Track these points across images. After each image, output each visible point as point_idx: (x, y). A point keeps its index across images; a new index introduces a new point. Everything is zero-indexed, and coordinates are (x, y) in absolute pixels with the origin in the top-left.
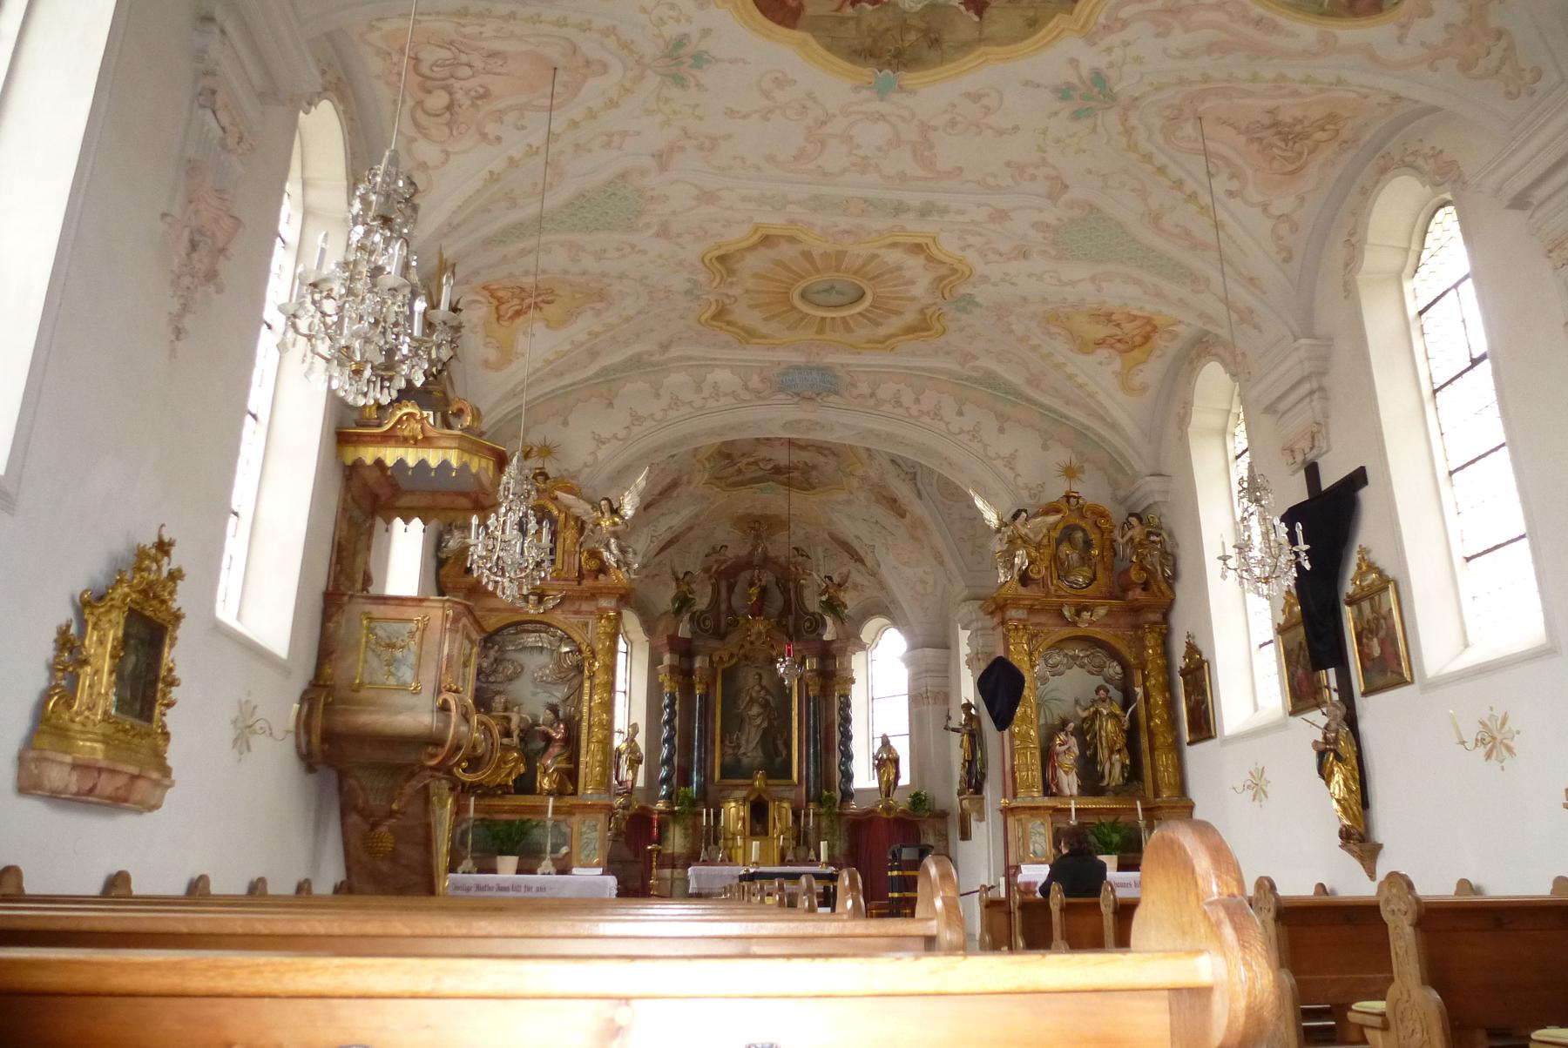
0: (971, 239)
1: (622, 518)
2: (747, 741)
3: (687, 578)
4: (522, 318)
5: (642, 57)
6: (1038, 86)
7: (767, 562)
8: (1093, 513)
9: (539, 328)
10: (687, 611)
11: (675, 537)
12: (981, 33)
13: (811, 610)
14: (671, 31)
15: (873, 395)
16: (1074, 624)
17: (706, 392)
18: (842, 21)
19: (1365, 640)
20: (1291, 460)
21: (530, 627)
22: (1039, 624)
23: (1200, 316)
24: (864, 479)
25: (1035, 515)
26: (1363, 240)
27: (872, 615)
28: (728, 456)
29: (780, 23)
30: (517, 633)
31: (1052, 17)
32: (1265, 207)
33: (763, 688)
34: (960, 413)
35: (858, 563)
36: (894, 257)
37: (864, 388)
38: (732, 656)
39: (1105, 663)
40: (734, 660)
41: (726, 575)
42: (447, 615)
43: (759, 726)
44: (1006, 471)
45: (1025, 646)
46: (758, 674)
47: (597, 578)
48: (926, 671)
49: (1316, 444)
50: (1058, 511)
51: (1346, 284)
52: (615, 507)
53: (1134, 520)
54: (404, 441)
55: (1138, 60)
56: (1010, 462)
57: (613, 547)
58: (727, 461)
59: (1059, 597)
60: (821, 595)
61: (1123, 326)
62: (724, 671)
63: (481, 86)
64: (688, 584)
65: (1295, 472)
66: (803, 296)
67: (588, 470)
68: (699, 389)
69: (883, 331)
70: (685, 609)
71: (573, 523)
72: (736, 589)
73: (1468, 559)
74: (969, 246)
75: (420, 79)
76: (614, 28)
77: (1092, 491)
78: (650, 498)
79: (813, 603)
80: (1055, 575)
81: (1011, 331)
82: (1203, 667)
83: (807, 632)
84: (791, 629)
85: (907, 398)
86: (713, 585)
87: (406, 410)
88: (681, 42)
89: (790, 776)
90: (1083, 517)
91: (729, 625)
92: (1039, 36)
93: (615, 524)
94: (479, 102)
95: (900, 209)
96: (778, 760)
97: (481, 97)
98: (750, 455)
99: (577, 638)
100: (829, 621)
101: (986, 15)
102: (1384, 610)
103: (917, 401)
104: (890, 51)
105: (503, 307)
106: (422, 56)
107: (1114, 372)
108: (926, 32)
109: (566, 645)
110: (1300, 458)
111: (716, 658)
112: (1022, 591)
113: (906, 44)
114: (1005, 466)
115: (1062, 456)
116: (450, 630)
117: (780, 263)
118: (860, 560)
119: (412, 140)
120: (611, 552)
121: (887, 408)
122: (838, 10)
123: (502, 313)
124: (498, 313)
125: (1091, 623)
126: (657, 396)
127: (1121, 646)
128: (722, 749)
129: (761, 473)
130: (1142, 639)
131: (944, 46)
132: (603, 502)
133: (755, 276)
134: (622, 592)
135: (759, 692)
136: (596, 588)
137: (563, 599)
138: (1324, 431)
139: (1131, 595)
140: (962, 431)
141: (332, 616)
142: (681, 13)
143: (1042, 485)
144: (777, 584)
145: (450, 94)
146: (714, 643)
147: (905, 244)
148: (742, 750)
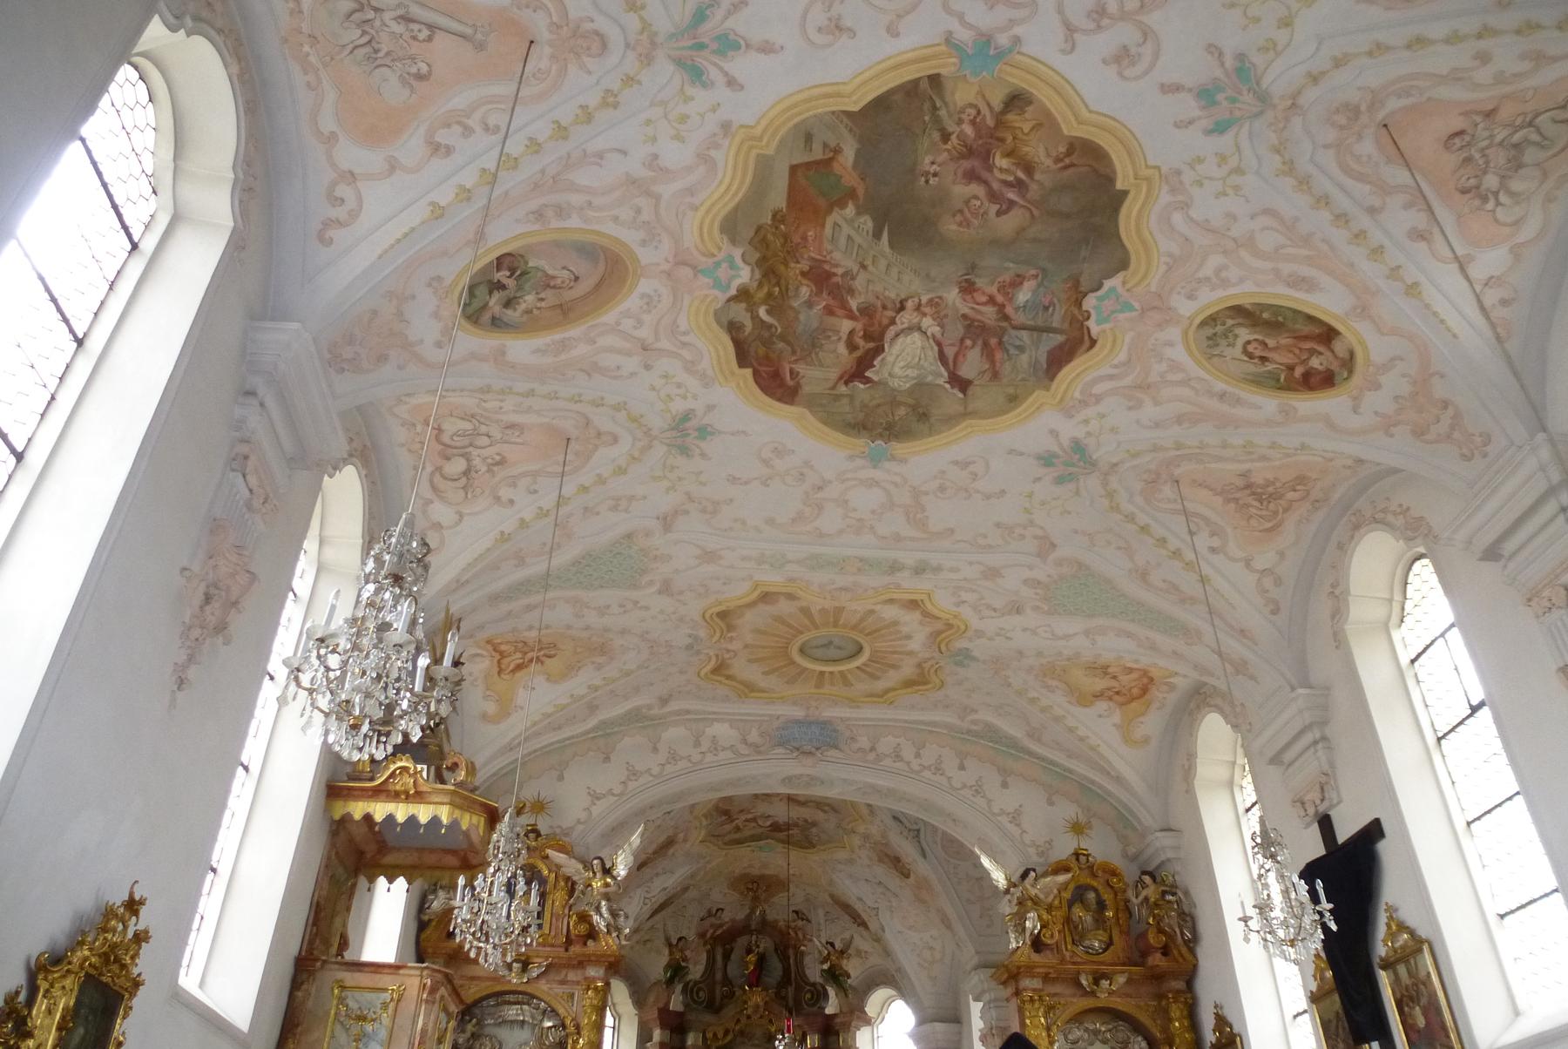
0: (965, 596)
1: (614, 878)
3: (681, 944)
5: (650, 430)
6: (1022, 454)
7: (765, 926)
8: (1104, 871)
9: (540, 680)
10: (679, 982)
11: (670, 898)
12: (965, 408)
13: (812, 980)
14: (678, 406)
15: (873, 749)
16: (1093, 994)
17: (705, 745)
18: (837, 397)
19: (1406, 1009)
20: (1303, 813)
21: (512, 998)
22: (1055, 995)
23: (1196, 667)
24: (866, 837)
25: (1045, 875)
26: (1347, 592)
27: (878, 985)
28: (726, 813)
29: (779, 400)
30: (498, 1005)
31: (1031, 394)
32: (1248, 563)
34: (962, 767)
35: (861, 928)
36: (890, 613)
37: (864, 742)
38: (727, 1032)
39: (1129, 1038)
40: (729, 1038)
41: (722, 940)
42: (425, 985)
44: (1011, 828)
45: (1042, 1020)
47: (585, 944)
49: (1327, 795)
50: (1067, 870)
51: (1335, 634)
52: (608, 867)
53: (1147, 879)
54: (396, 796)
55: (1113, 430)
56: (1016, 817)
57: (604, 910)
58: (724, 818)
59: (1074, 963)
60: (822, 963)
61: (1121, 678)
63: (498, 454)
64: (682, 951)
65: (1308, 825)
66: (802, 651)
67: (581, 827)
68: (697, 744)
69: (881, 685)
70: (677, 979)
71: (562, 884)
72: (733, 957)
73: (1502, 917)
74: (964, 602)
75: (441, 447)
76: (625, 403)
77: (1101, 847)
78: (644, 857)
79: (814, 972)
80: (1069, 939)
81: (1009, 685)
82: (1235, 1042)
84: (791, 1003)
85: (908, 753)
86: (708, 952)
87: (400, 764)
88: (687, 416)
90: (1094, 876)
91: (724, 997)
92: (1018, 411)
93: (607, 885)
94: (495, 468)
95: (894, 567)
97: (497, 464)
98: (749, 812)
99: (561, 1011)
100: (831, 992)
101: (970, 392)
102: (1422, 974)
103: (918, 755)
104: (882, 424)
105: (505, 661)
106: (445, 426)
107: (1115, 725)
108: (914, 408)
109: (549, 1020)
110: (1311, 811)
111: (710, 1035)
112: (1036, 957)
113: (897, 418)
114: (1011, 822)
115: (1069, 810)
116: (427, 1001)
117: (779, 619)
118: (864, 924)
119: (429, 502)
120: (601, 915)
121: (887, 762)
122: (833, 388)
123: (503, 666)
124: (499, 667)
125: (1111, 993)
126: (655, 750)
127: (1144, 1018)
129: (760, 830)
130: (1166, 1011)
131: (932, 420)
132: (595, 862)
133: (758, 631)
134: (612, 959)
136: (584, 955)
137: (549, 967)
138: (1332, 782)
139: (1151, 961)
140: (964, 786)
141: (302, 983)
142: (687, 391)
143: (1050, 842)
144: (776, 950)
145: (468, 460)
146: (708, 1018)
147: (900, 600)
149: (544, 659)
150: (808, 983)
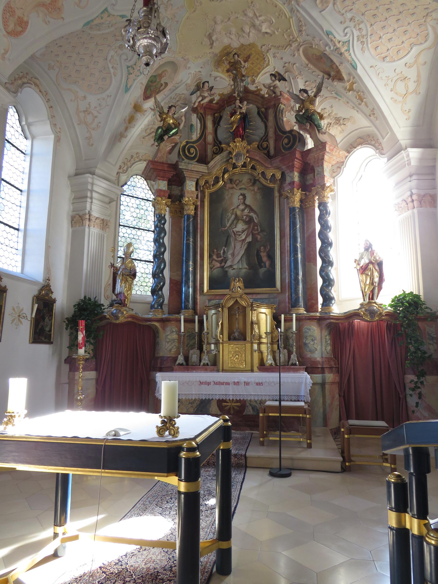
2: (233, 255)
33: (247, 206)
43: (244, 240)
46: (241, 195)
48: (411, 176)
62: (211, 195)
72: (222, 123)
83: (284, 148)
84: (272, 152)
89: (273, 285)
96: (262, 271)
111: (202, 183)
128: (210, 263)
135: (243, 210)
144: (259, 113)
148: (229, 263)
150: (284, 132)
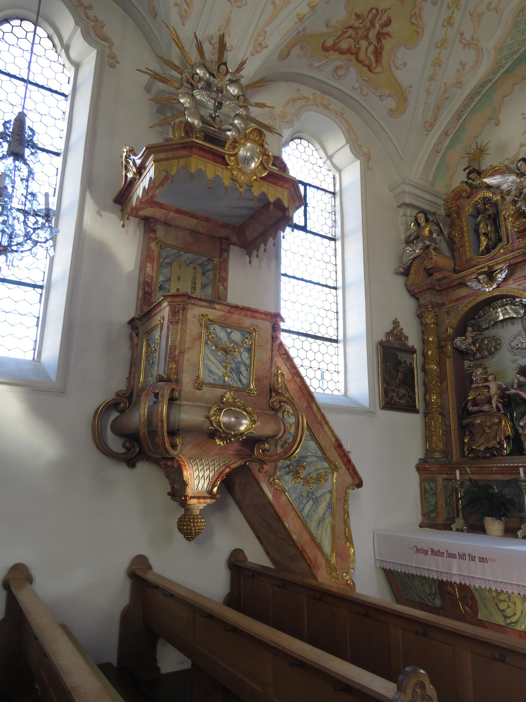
4: (385, 54)
105: (362, 56)
123: (367, 62)
124: (365, 65)
149: (385, 30)
